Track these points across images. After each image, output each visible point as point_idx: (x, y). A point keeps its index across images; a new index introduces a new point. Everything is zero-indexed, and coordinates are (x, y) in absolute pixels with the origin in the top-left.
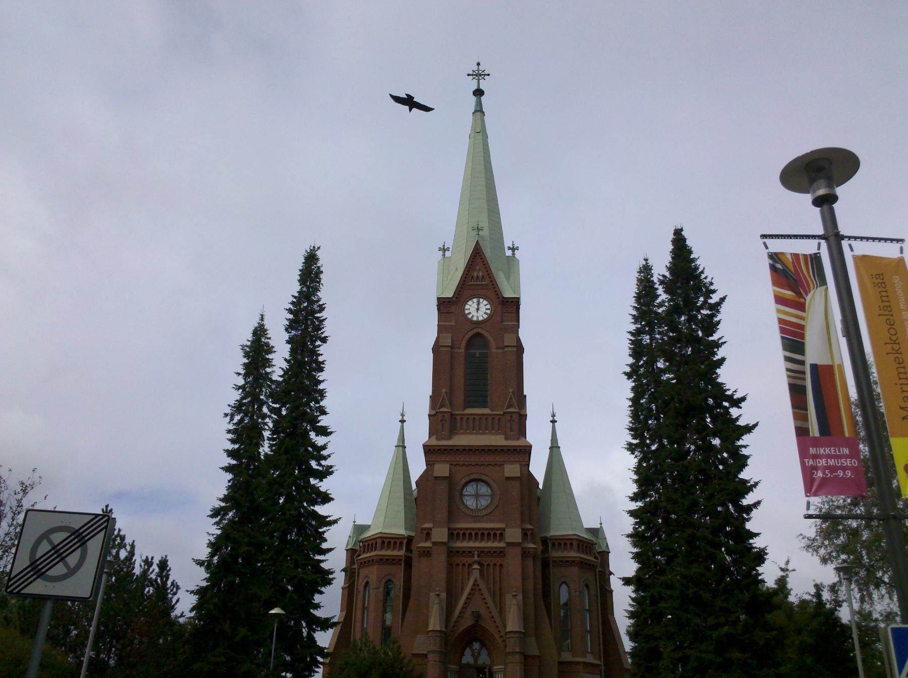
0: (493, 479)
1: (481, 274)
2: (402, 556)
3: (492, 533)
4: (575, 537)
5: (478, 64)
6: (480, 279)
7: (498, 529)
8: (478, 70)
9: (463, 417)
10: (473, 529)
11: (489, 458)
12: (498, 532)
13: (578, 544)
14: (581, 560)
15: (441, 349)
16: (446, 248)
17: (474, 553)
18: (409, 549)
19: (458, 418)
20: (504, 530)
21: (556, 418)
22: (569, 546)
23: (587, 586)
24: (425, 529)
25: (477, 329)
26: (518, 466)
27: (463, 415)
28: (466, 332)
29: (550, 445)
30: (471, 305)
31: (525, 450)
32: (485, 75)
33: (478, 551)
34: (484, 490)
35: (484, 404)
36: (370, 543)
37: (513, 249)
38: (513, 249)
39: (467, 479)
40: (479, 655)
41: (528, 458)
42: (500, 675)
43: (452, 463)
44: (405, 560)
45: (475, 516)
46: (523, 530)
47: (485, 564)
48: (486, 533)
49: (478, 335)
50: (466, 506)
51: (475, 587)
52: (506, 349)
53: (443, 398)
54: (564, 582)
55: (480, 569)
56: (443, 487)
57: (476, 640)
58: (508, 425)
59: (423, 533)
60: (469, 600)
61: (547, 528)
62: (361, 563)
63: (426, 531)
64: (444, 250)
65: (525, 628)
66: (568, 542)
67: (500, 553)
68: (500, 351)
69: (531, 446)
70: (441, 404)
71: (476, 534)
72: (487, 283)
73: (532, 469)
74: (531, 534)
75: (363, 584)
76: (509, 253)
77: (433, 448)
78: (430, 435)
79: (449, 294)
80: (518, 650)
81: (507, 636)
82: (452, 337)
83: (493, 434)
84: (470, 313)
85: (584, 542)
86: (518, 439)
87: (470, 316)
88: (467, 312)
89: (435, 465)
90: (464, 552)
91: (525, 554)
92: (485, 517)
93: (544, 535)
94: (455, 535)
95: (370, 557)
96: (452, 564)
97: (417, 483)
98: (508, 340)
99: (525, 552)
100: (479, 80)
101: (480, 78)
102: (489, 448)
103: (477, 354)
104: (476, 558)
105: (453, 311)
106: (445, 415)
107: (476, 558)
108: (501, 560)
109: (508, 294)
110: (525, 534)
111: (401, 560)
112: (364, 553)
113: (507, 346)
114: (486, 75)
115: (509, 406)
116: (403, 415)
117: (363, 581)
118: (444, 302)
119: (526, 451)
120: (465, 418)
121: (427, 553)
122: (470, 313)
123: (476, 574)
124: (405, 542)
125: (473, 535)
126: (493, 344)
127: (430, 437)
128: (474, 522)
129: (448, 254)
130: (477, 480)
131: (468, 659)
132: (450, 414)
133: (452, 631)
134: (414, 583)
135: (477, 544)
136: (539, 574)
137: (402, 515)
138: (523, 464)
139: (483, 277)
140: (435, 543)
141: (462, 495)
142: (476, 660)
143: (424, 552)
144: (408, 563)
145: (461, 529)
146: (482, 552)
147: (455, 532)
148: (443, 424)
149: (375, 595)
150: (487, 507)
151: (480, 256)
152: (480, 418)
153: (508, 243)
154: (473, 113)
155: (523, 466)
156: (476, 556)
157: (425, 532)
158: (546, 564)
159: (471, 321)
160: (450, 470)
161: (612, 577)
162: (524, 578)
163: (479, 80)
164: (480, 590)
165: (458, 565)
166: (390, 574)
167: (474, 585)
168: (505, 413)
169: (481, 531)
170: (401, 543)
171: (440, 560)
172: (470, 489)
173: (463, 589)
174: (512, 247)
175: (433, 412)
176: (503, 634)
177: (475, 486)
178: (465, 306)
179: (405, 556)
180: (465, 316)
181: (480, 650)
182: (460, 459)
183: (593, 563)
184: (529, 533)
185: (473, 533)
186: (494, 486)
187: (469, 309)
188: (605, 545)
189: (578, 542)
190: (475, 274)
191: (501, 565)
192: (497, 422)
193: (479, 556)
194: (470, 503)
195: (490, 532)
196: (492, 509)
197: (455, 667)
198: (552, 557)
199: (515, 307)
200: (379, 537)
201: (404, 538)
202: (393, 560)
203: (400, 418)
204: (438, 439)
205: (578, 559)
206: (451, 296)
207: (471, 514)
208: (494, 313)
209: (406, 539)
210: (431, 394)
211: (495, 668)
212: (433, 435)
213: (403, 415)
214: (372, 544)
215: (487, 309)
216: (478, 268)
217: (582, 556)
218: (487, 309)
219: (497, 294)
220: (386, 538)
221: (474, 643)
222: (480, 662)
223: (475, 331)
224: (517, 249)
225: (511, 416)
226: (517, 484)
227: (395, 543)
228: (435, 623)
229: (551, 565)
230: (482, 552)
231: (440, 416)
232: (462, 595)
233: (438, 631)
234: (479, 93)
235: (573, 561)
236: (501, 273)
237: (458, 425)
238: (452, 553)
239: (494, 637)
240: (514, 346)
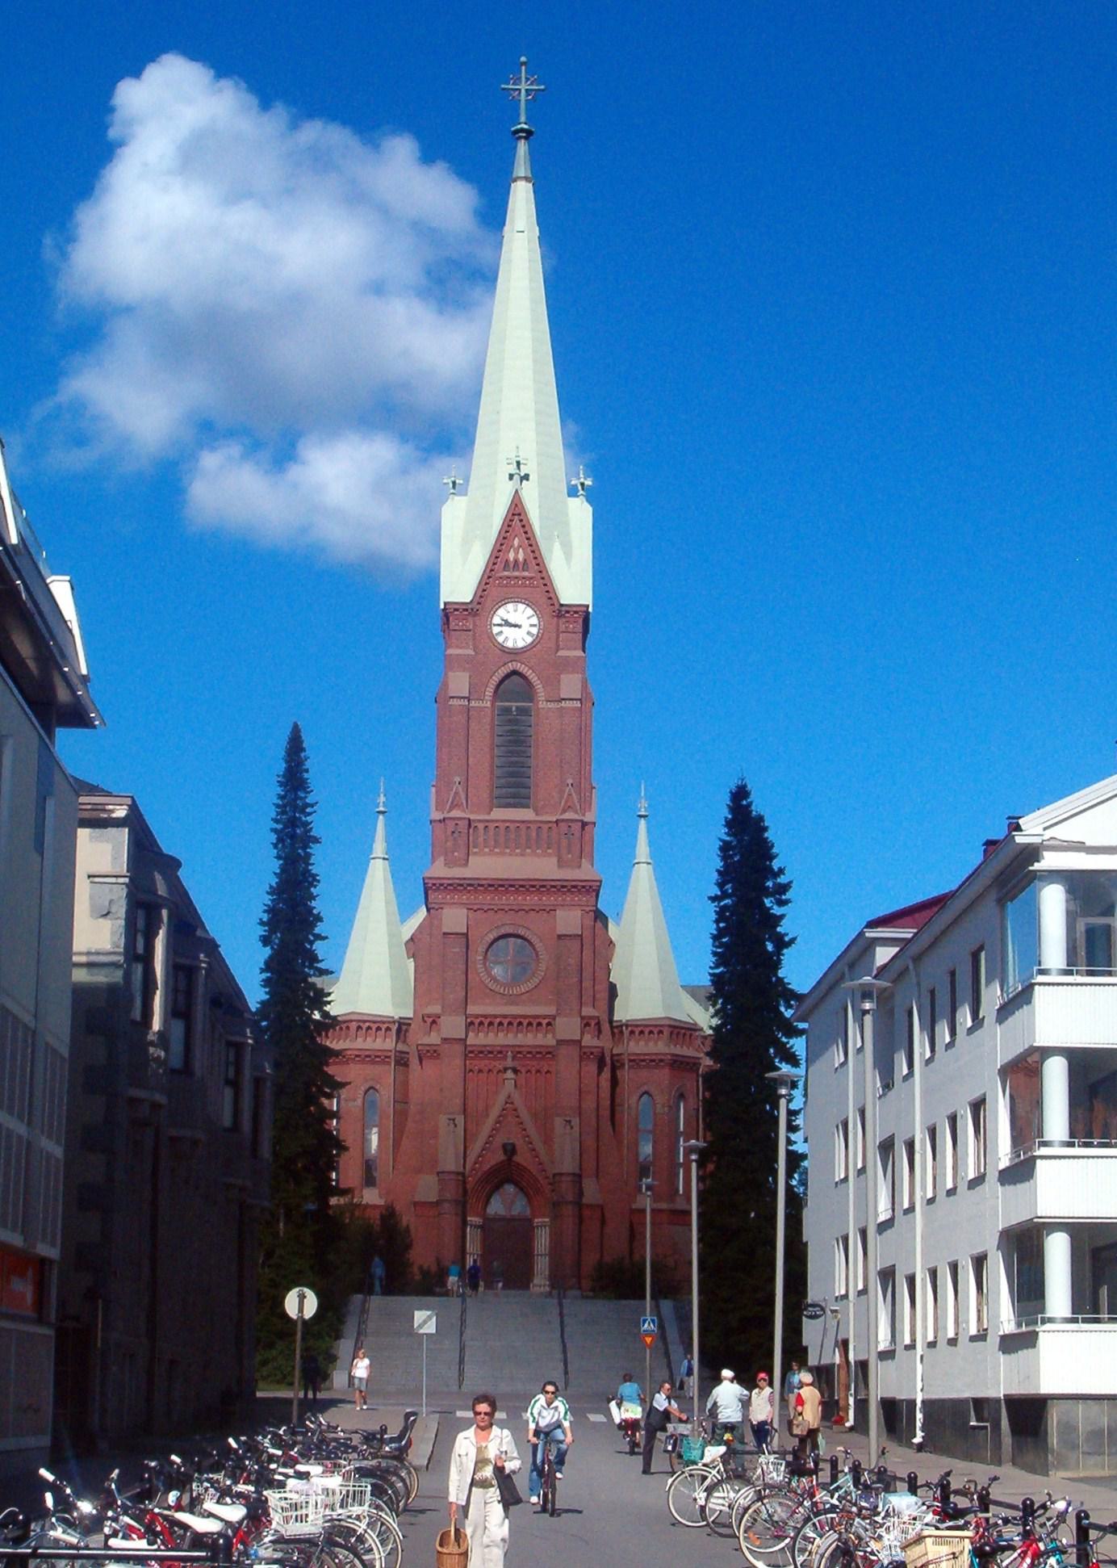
0: (536, 934)
1: (521, 557)
4: (668, 1023)
7: (545, 1017)
11: (532, 900)
13: (671, 1033)
14: (675, 1058)
15: (451, 702)
19: (481, 826)
24: (429, 1016)
25: (514, 663)
26: (579, 913)
27: (487, 821)
31: (590, 887)
40: (512, 1203)
44: (395, 1056)
46: (582, 1018)
47: (523, 1070)
52: (563, 704)
53: (456, 793)
56: (457, 949)
58: (564, 842)
59: (425, 1022)
63: (431, 1020)
67: (547, 1054)
70: (452, 803)
72: (533, 575)
77: (439, 882)
80: (571, 1199)
82: (470, 677)
83: (538, 856)
89: (445, 911)
92: (523, 997)
103: (514, 709)
104: (509, 1059)
105: (471, 627)
107: (509, 1063)
111: (389, 1057)
113: (563, 699)
120: (492, 826)
123: (510, 1084)
124: (395, 1028)
128: (506, 1004)
138: (588, 909)
144: (402, 1061)
146: (518, 1052)
148: (455, 839)
151: (521, 521)
166: (372, 1079)
167: (506, 1103)
182: (486, 899)
189: (671, 1029)
190: (511, 556)
193: (514, 1058)
198: (629, 1054)
201: (394, 1022)
202: (377, 1057)
205: (669, 1057)
206: (468, 601)
208: (543, 634)
209: (397, 1024)
211: (536, 1220)
215: (531, 625)
216: (516, 542)
218: (531, 625)
219: (550, 598)
223: (511, 667)
226: (575, 945)
229: (627, 1067)
231: (451, 826)
233: (453, 1172)
235: (661, 1061)
236: (557, 546)
237: (481, 839)
238: (471, 1053)
239: (537, 1179)
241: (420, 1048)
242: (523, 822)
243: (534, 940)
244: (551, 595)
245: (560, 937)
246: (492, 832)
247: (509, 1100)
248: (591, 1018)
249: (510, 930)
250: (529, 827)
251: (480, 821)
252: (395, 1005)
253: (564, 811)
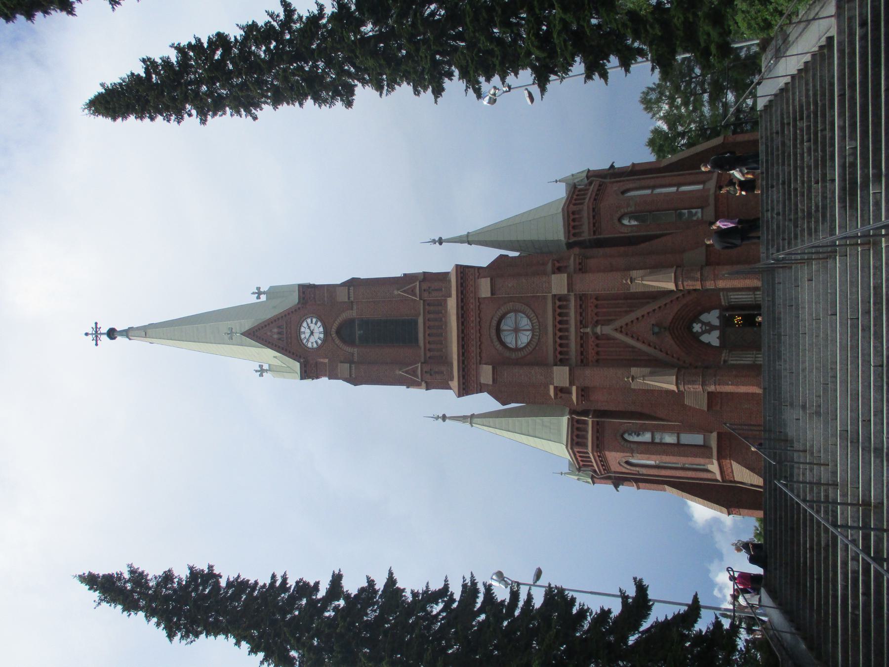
1: (275, 330)
2: (593, 421)
3: (558, 311)
5: (87, 334)
6: (281, 330)
7: (554, 303)
8: (92, 334)
9: (427, 349)
10: (555, 334)
12: (558, 303)
13: (574, 204)
15: (353, 376)
16: (259, 369)
17: (584, 333)
18: (585, 413)
19: (428, 355)
20: (555, 295)
21: (437, 239)
22: (577, 216)
23: (623, 193)
24: (556, 394)
25: (332, 333)
27: (425, 349)
28: (336, 346)
29: (466, 245)
31: (461, 273)
32: (96, 327)
33: (581, 328)
34: (508, 324)
35: (413, 323)
36: (579, 458)
39: (497, 343)
40: (708, 324)
41: (470, 269)
42: (732, 297)
43: (478, 361)
44: (598, 417)
45: (538, 330)
48: (558, 318)
49: (338, 332)
50: (528, 344)
51: (623, 330)
54: (620, 220)
55: (602, 325)
57: (690, 328)
59: (561, 397)
60: (640, 338)
61: (557, 242)
62: (604, 470)
65: (672, 267)
66: (572, 217)
67: (582, 298)
68: (355, 307)
69: (457, 266)
71: (560, 330)
73: (485, 264)
74: (558, 261)
75: (628, 467)
76: (263, 298)
78: (448, 387)
79: (297, 366)
80: (699, 274)
81: (682, 289)
84: (316, 342)
85: (572, 197)
86: (450, 281)
87: (320, 342)
88: (315, 345)
90: (582, 346)
91: (582, 269)
93: (565, 247)
94: (562, 357)
95: (595, 460)
96: (597, 361)
97: (504, 404)
98: (342, 297)
99: (580, 269)
100: (101, 334)
101: (99, 332)
102: (460, 316)
104: (588, 330)
106: (424, 370)
108: (591, 298)
109: (294, 299)
110: (559, 270)
112: (593, 466)
113: (349, 298)
115: (413, 292)
116: (437, 418)
117: (625, 468)
118: (305, 372)
119: (463, 271)
120: (428, 346)
121: (584, 392)
122: (316, 342)
123: (607, 330)
125: (561, 334)
126: (345, 316)
127: (450, 389)
129: (266, 367)
130: (498, 330)
131: (713, 339)
132: (424, 365)
133: (678, 359)
134: (621, 408)
135: (573, 329)
136: (608, 250)
137: (546, 419)
139: (279, 327)
140: (572, 383)
141: (517, 349)
142: (712, 328)
143: (582, 396)
145: (555, 350)
146: (582, 323)
147: (559, 357)
149: (641, 453)
150: (528, 317)
152: (428, 327)
154: (130, 339)
155: (479, 274)
156: (588, 330)
157: (560, 394)
158: (600, 243)
159: (324, 341)
160: (485, 364)
161: (616, 165)
162: (612, 269)
164: (627, 324)
165: (598, 353)
167: (621, 332)
168: (420, 299)
169: (557, 324)
170: (578, 421)
171: (593, 376)
172: (509, 340)
173: (627, 346)
174: (256, 295)
175: (424, 384)
176: (680, 294)
177: (506, 333)
179: (593, 417)
180: (320, 347)
181: (703, 323)
183: (597, 186)
184: (557, 265)
185: (559, 334)
186: (503, 310)
187: (312, 343)
188: (580, 175)
190: (275, 336)
191: (597, 299)
192: (432, 308)
193: (586, 327)
194: (524, 339)
195: (557, 313)
196: (531, 312)
197: (723, 355)
199: (309, 290)
200: (572, 449)
201: (572, 419)
203: (440, 420)
204: (452, 379)
206: (298, 365)
207: (537, 337)
210: (405, 387)
211: (723, 303)
212: (449, 384)
214: (580, 456)
215: (312, 322)
217: (587, 200)
218: (312, 322)
220: (572, 440)
221: (695, 330)
222: (716, 322)
223: (334, 335)
225: (424, 290)
227: (578, 429)
228: (667, 384)
229: (599, 236)
230: (581, 322)
231: (427, 377)
232: (633, 347)
234: (112, 334)
240: (349, 290)
241: (580, 402)
242: (424, 324)
243: (500, 313)
244: (293, 310)
245: (492, 294)
246: (432, 346)
247: (620, 330)
248: (553, 265)
249: (493, 332)
250: (428, 320)
251: (425, 354)
252: (563, 415)
253: (415, 295)
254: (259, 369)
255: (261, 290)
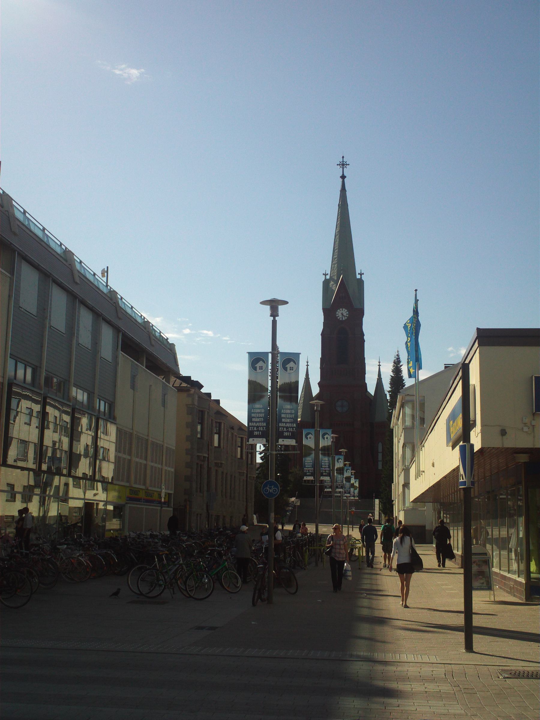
5: (343, 157)
8: (343, 161)
16: (326, 273)
30: (339, 312)
32: (347, 165)
37: (361, 274)
38: (361, 274)
64: (325, 275)
76: (358, 277)
88: (337, 316)
100: (343, 168)
114: (347, 165)
153: (358, 271)
159: (339, 320)
163: (343, 168)
178: (336, 312)
180: (337, 317)
210: (321, 357)
213: (307, 362)
224: (363, 274)
234: (343, 177)
254: (326, 273)
255: (362, 275)
